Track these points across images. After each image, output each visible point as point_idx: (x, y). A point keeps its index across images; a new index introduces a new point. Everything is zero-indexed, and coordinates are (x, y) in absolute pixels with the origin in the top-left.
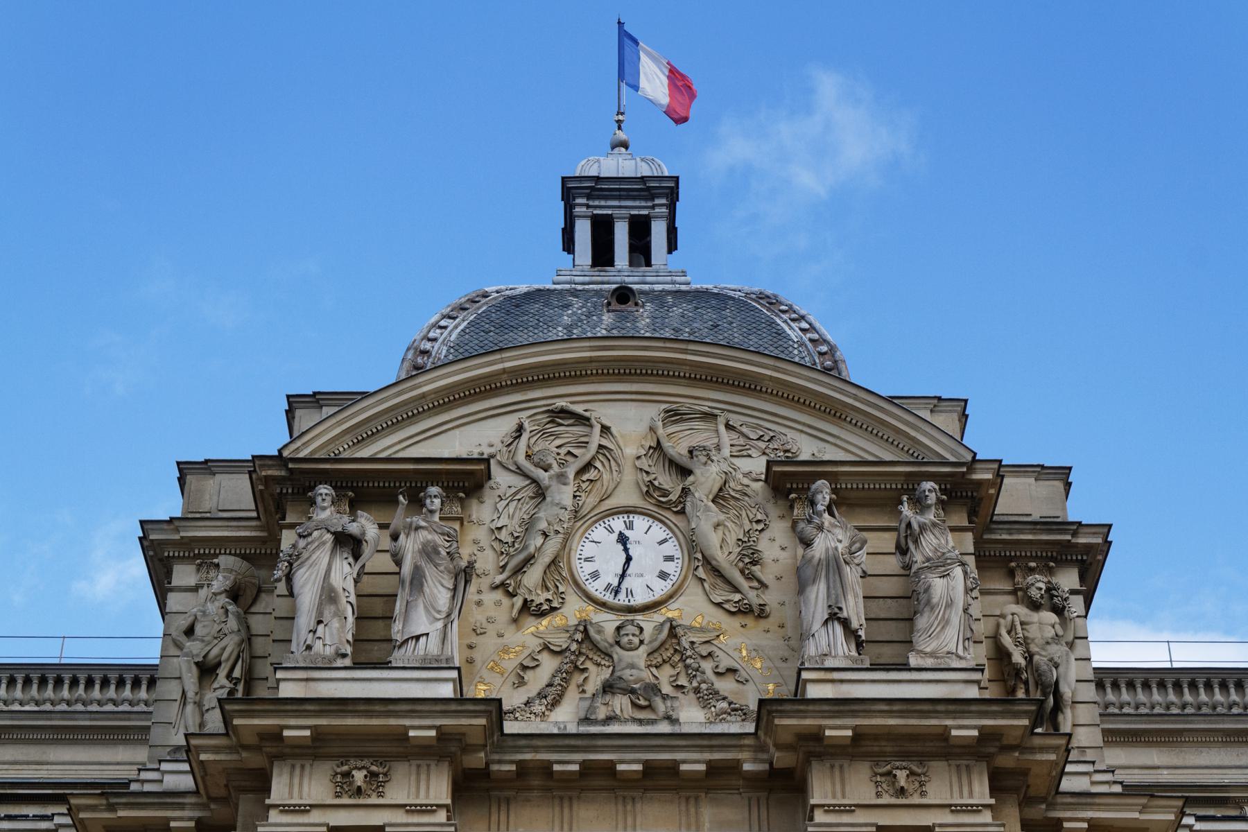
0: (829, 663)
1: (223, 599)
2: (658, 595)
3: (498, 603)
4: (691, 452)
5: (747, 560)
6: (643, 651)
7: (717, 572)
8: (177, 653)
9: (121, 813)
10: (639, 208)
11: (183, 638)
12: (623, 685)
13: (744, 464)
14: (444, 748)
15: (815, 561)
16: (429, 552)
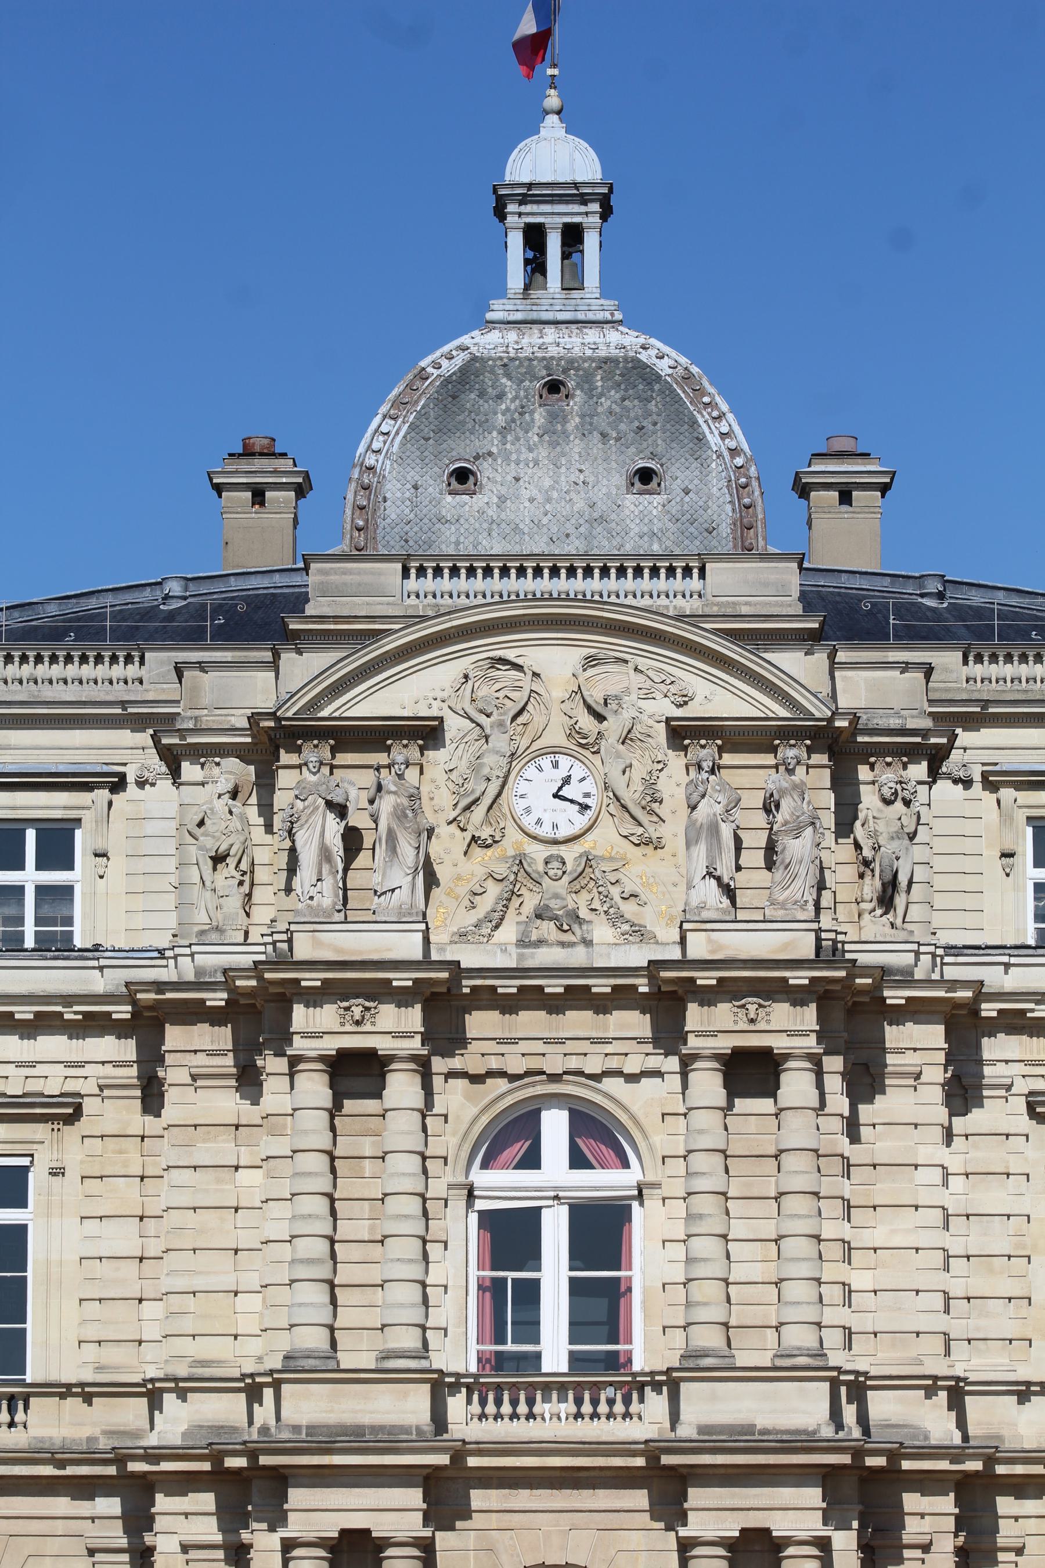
0: (705, 915)
2: (575, 830)
3: (452, 836)
4: (606, 700)
5: (649, 799)
6: (566, 879)
7: (623, 806)
8: (195, 842)
12: (549, 914)
15: (698, 824)
16: (399, 814)
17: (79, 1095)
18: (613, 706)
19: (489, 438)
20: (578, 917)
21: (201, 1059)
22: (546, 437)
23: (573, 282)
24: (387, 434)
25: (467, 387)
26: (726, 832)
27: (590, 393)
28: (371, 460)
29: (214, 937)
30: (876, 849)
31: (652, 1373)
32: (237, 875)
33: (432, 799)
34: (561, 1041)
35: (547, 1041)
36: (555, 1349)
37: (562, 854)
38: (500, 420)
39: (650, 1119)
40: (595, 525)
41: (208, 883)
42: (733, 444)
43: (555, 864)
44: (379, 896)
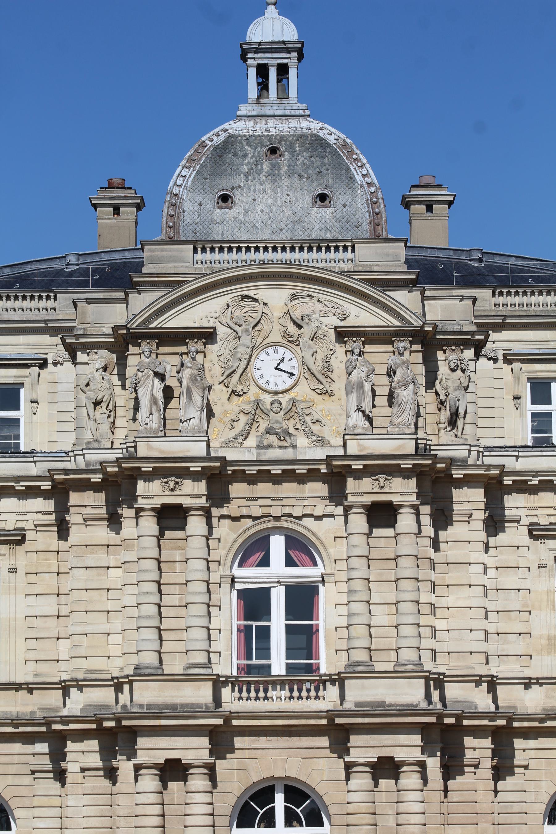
0: (357, 431)
2: (287, 386)
3: (221, 390)
4: (302, 317)
5: (326, 369)
6: (282, 413)
7: (312, 374)
8: (84, 394)
9: (72, 476)
12: (273, 431)
13: (325, 320)
15: (352, 383)
16: (193, 379)
17: (24, 530)
18: (306, 320)
19: (239, 178)
20: (289, 433)
21: (89, 510)
22: (270, 178)
23: (283, 94)
24: (185, 176)
25: (227, 151)
26: (367, 387)
27: (293, 154)
28: (176, 190)
29: (95, 445)
30: (447, 395)
31: (330, 675)
32: (107, 412)
33: (210, 371)
34: (280, 499)
35: (273, 499)
36: (278, 663)
37: (280, 399)
38: (245, 168)
39: (328, 540)
40: (296, 224)
41: (91, 416)
42: (369, 180)
43: (276, 405)
44: (183, 423)
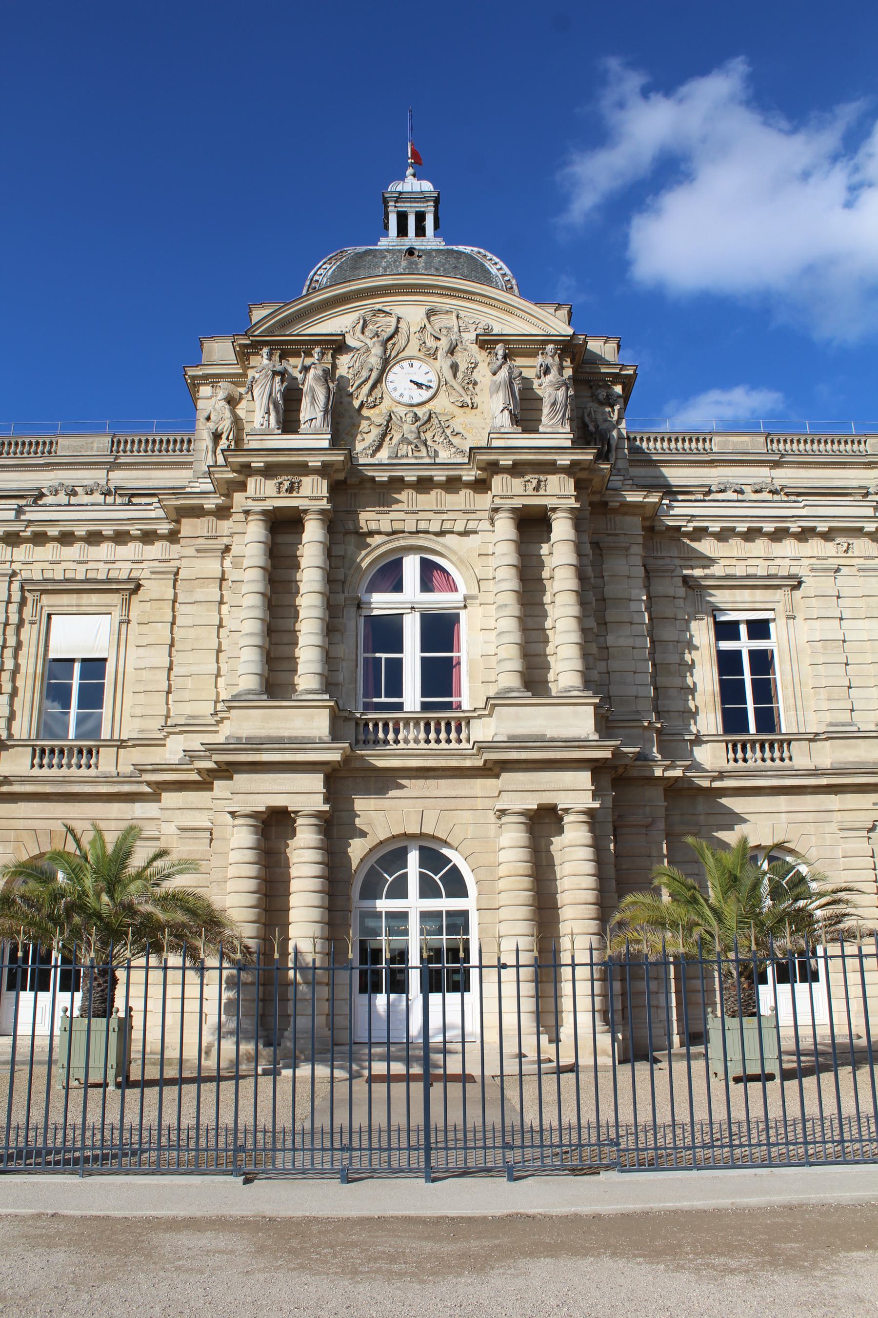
0: (503, 430)
1: (223, 403)
5: (466, 382)
10: (420, 207)
11: (204, 421)
14: (324, 470)
18: (444, 332)
21: (201, 541)
23: (420, 231)
